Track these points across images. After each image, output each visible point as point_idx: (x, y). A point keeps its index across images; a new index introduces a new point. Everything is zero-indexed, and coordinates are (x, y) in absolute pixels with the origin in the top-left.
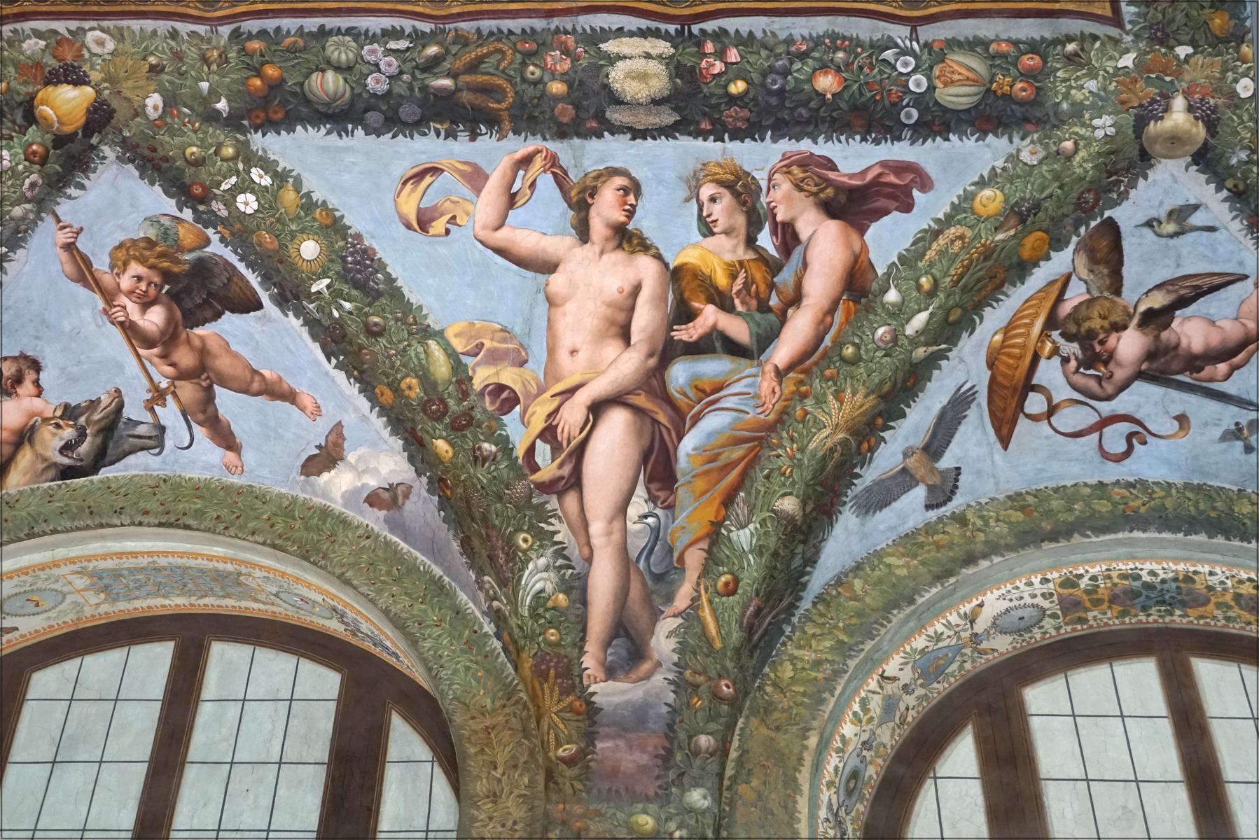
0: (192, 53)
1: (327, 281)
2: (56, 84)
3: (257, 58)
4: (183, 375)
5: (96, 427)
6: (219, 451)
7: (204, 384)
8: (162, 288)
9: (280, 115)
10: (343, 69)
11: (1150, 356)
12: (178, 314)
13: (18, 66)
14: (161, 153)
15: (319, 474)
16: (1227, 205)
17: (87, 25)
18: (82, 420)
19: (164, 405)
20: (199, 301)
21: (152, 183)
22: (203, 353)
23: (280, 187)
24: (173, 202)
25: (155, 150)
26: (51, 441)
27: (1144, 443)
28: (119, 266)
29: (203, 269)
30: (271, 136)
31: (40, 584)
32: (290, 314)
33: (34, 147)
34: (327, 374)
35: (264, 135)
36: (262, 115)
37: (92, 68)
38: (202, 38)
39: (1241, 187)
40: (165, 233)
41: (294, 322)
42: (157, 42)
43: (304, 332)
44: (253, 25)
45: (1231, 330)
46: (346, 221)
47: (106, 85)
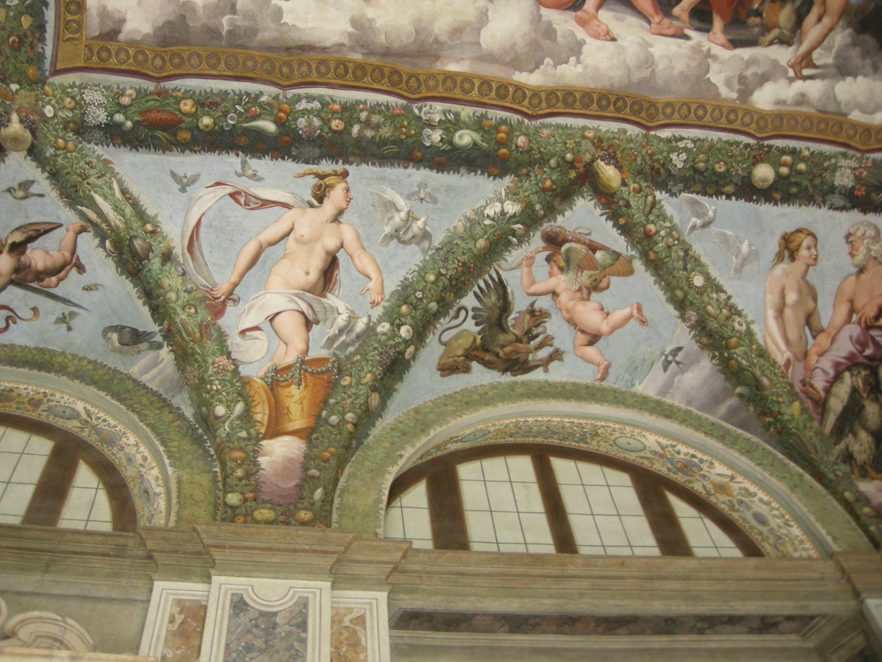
11: (17, 270)
16: (48, 181)
27: (15, 323)
39: (54, 171)
45: (57, 257)
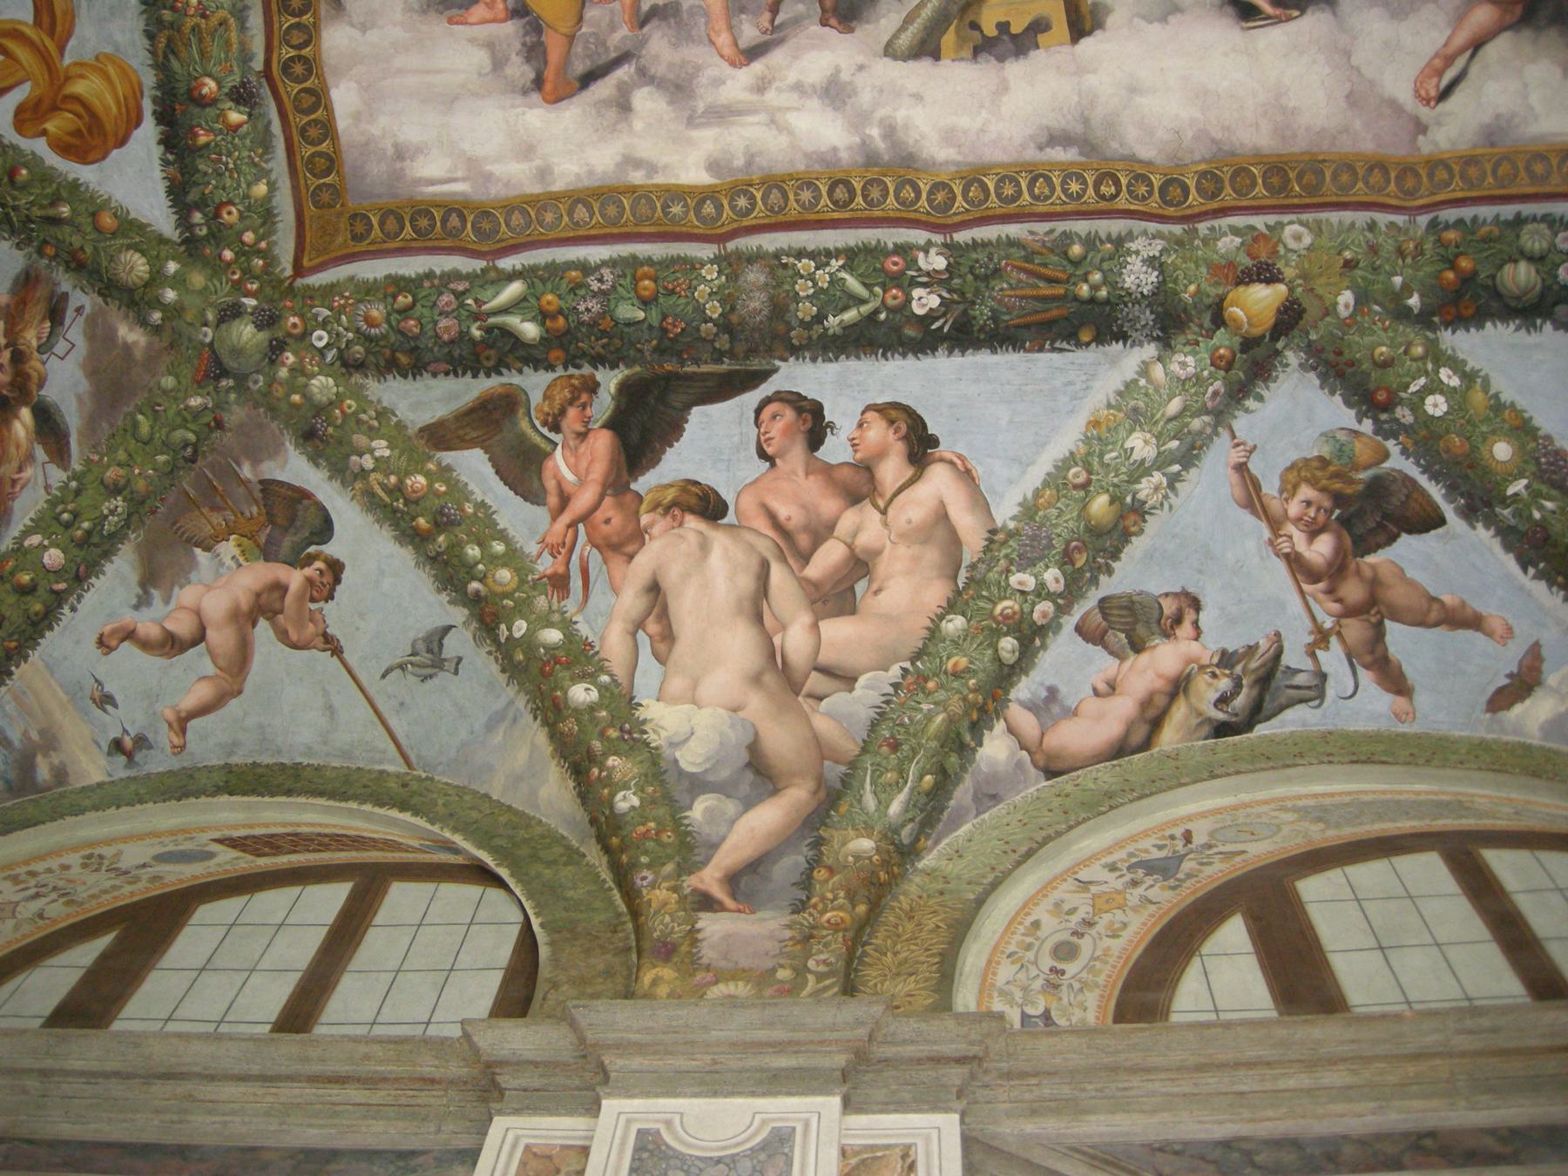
0: (1388, 246)
1: (1524, 482)
2: (1247, 284)
3: (1452, 249)
4: (1351, 612)
5: (1253, 677)
6: (1388, 698)
7: (1373, 620)
8: (1332, 512)
9: (1471, 311)
10: (1536, 259)
12: (1348, 541)
13: (1211, 266)
14: (1347, 355)
15: (1509, 707)
17: (1286, 218)
18: (1238, 669)
19: (1327, 648)
20: (1372, 525)
21: (1332, 393)
22: (1374, 583)
23: (1469, 388)
24: (1352, 413)
25: (1339, 353)
26: (1207, 691)
28: (1289, 489)
29: (1378, 488)
30: (1460, 334)
31: (1241, 820)
32: (1479, 526)
33: (1222, 351)
34: (1522, 588)
35: (1454, 332)
36: (1453, 310)
37: (1287, 265)
38: (1399, 229)
40: (1340, 450)
41: (1483, 534)
42: (1354, 235)
43: (1496, 545)
44: (1449, 215)
46: (1537, 422)
47: (1300, 281)
